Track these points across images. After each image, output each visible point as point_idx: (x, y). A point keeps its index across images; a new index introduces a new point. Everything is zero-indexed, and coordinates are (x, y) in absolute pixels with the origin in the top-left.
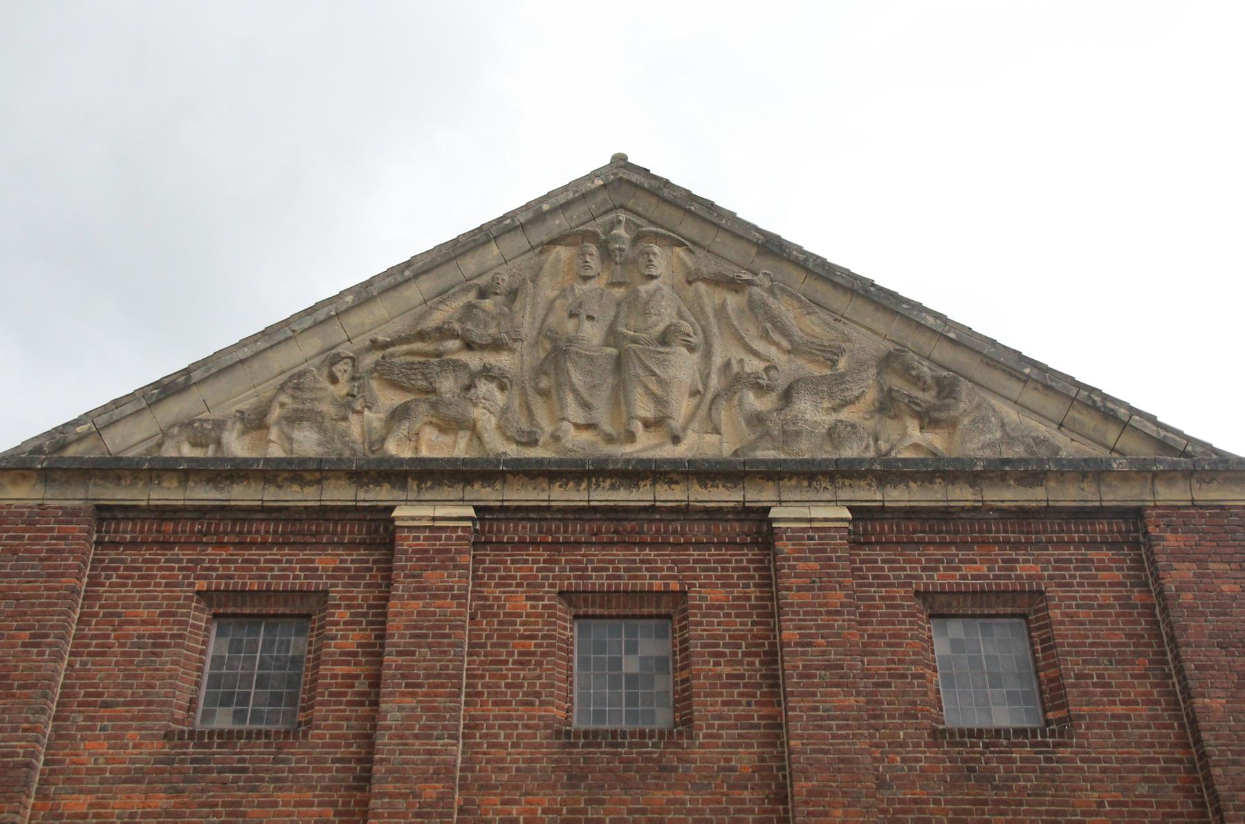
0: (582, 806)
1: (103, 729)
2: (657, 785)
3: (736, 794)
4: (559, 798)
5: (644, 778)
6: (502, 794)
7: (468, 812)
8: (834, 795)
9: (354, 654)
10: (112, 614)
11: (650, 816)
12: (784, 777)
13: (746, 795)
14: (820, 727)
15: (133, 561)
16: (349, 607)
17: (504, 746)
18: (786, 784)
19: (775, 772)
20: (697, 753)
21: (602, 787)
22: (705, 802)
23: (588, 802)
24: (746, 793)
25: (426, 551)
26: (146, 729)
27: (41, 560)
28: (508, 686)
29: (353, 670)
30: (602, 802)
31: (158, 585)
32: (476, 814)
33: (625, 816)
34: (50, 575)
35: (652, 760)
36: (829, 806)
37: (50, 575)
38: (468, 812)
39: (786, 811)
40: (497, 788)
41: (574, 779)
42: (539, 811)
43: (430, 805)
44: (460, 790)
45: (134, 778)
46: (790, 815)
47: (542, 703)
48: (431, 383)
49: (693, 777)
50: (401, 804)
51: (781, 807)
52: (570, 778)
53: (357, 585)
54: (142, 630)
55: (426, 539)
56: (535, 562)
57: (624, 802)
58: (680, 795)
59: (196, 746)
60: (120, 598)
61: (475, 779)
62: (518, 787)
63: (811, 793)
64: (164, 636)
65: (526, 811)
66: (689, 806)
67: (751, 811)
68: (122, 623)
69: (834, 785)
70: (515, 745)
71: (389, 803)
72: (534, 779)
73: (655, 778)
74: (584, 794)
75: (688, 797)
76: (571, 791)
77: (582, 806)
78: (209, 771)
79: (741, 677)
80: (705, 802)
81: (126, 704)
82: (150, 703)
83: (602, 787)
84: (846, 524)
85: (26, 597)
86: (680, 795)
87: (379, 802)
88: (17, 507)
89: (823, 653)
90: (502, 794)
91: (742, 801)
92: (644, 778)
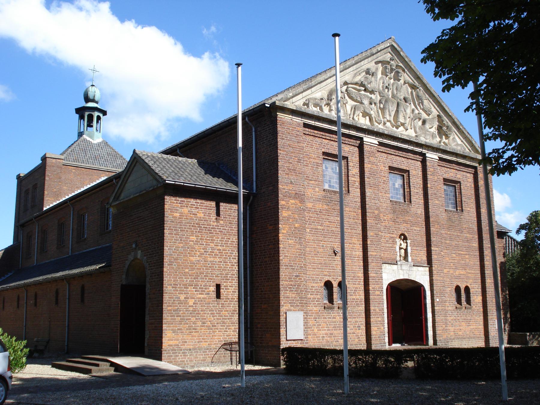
1: (311, 187)
9: (354, 175)
10: (307, 155)
14: (433, 207)
15: (308, 140)
16: (352, 162)
17: (382, 203)
20: (412, 209)
25: (369, 152)
26: (319, 188)
27: (295, 137)
28: (382, 188)
29: (355, 179)
31: (315, 148)
34: (298, 142)
35: (405, 209)
37: (298, 142)
41: (394, 212)
45: (319, 200)
47: (388, 193)
48: (361, 100)
52: (393, 212)
53: (353, 157)
54: (314, 160)
55: (370, 148)
56: (384, 157)
59: (329, 194)
60: (308, 150)
62: (385, 213)
64: (318, 163)
68: (310, 158)
70: (384, 203)
78: (332, 201)
79: (418, 193)
81: (314, 181)
82: (319, 181)
84: (437, 161)
85: (295, 148)
88: (286, 119)
89: (434, 191)
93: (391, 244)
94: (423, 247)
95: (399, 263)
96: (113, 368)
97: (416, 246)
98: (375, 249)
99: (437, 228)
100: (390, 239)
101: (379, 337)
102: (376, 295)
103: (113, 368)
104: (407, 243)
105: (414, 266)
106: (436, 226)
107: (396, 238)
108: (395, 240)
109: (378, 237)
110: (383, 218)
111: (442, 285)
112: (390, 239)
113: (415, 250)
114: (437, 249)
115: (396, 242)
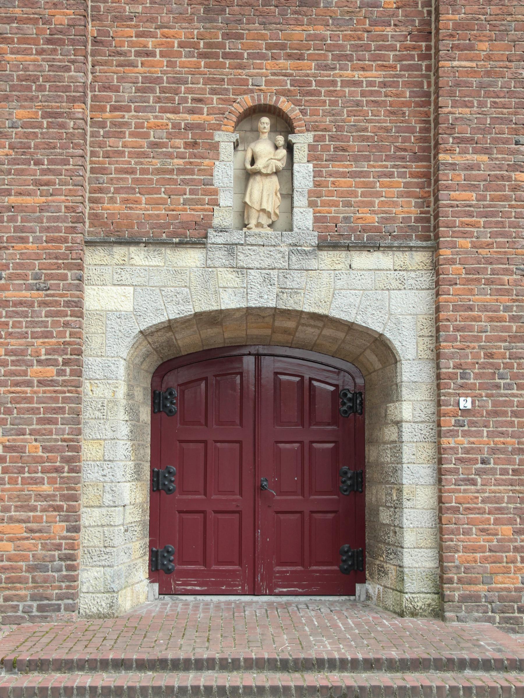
0: (220, 40)
2: (296, 19)
3: (378, 30)
4: (196, 32)
5: (283, 14)
6: (136, 26)
7: (101, 43)
8: (481, 28)
11: (288, 51)
12: (429, 13)
13: (389, 31)
18: (430, 20)
19: (420, 8)
21: (240, 21)
22: (346, 38)
23: (227, 36)
24: (388, 29)
30: (240, 37)
32: (111, 45)
33: (264, 51)
36: (475, 39)
38: (101, 43)
39: (428, 48)
40: (131, 19)
42: (176, 45)
43: (61, 32)
44: (93, 20)
46: (433, 52)
49: (334, 12)
50: (31, 30)
51: (424, 44)
52: (207, 11)
57: (262, 37)
58: (321, 30)
61: (108, 11)
62: (152, 20)
63: (457, 26)
65: (161, 44)
66: (329, 42)
67: (392, 48)
69: (483, 17)
71: (17, 28)
72: (170, 12)
73: (295, 13)
74: (221, 29)
75: (328, 33)
76: (208, 25)
77: (220, 40)
80: (346, 38)
83: (240, 21)
86: (321, 30)
87: (8, 27)
90: (136, 26)
91: (384, 38)
92: (283, 14)
93: (181, 156)
94: (403, 158)
95: (214, 237)
96: (358, 586)
97: (356, 159)
98: (38, 183)
99: (489, 58)
100: (170, 136)
101: (31, 569)
102: (29, 384)
103: (358, 586)
104: (290, 147)
105: (320, 247)
106: (485, 46)
107: (218, 127)
108: (211, 136)
109: (62, 126)
110: (132, 44)
111: (507, 329)
112: (170, 136)
113: (343, 175)
114: (485, 158)
115: (215, 147)
